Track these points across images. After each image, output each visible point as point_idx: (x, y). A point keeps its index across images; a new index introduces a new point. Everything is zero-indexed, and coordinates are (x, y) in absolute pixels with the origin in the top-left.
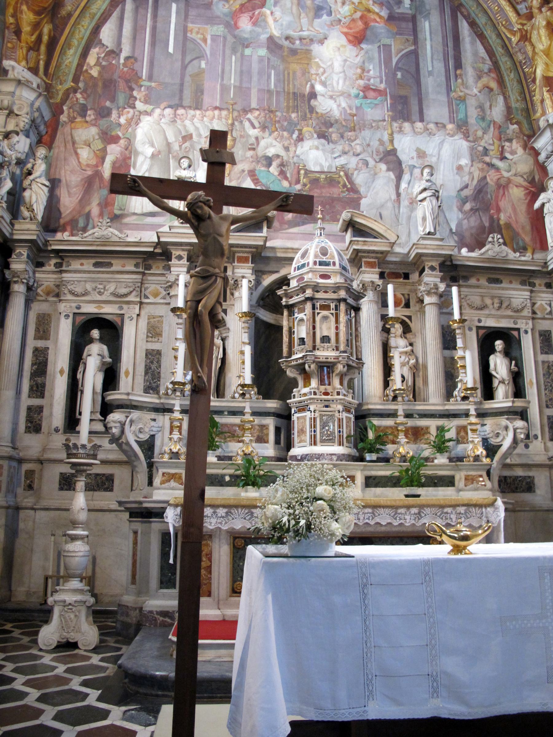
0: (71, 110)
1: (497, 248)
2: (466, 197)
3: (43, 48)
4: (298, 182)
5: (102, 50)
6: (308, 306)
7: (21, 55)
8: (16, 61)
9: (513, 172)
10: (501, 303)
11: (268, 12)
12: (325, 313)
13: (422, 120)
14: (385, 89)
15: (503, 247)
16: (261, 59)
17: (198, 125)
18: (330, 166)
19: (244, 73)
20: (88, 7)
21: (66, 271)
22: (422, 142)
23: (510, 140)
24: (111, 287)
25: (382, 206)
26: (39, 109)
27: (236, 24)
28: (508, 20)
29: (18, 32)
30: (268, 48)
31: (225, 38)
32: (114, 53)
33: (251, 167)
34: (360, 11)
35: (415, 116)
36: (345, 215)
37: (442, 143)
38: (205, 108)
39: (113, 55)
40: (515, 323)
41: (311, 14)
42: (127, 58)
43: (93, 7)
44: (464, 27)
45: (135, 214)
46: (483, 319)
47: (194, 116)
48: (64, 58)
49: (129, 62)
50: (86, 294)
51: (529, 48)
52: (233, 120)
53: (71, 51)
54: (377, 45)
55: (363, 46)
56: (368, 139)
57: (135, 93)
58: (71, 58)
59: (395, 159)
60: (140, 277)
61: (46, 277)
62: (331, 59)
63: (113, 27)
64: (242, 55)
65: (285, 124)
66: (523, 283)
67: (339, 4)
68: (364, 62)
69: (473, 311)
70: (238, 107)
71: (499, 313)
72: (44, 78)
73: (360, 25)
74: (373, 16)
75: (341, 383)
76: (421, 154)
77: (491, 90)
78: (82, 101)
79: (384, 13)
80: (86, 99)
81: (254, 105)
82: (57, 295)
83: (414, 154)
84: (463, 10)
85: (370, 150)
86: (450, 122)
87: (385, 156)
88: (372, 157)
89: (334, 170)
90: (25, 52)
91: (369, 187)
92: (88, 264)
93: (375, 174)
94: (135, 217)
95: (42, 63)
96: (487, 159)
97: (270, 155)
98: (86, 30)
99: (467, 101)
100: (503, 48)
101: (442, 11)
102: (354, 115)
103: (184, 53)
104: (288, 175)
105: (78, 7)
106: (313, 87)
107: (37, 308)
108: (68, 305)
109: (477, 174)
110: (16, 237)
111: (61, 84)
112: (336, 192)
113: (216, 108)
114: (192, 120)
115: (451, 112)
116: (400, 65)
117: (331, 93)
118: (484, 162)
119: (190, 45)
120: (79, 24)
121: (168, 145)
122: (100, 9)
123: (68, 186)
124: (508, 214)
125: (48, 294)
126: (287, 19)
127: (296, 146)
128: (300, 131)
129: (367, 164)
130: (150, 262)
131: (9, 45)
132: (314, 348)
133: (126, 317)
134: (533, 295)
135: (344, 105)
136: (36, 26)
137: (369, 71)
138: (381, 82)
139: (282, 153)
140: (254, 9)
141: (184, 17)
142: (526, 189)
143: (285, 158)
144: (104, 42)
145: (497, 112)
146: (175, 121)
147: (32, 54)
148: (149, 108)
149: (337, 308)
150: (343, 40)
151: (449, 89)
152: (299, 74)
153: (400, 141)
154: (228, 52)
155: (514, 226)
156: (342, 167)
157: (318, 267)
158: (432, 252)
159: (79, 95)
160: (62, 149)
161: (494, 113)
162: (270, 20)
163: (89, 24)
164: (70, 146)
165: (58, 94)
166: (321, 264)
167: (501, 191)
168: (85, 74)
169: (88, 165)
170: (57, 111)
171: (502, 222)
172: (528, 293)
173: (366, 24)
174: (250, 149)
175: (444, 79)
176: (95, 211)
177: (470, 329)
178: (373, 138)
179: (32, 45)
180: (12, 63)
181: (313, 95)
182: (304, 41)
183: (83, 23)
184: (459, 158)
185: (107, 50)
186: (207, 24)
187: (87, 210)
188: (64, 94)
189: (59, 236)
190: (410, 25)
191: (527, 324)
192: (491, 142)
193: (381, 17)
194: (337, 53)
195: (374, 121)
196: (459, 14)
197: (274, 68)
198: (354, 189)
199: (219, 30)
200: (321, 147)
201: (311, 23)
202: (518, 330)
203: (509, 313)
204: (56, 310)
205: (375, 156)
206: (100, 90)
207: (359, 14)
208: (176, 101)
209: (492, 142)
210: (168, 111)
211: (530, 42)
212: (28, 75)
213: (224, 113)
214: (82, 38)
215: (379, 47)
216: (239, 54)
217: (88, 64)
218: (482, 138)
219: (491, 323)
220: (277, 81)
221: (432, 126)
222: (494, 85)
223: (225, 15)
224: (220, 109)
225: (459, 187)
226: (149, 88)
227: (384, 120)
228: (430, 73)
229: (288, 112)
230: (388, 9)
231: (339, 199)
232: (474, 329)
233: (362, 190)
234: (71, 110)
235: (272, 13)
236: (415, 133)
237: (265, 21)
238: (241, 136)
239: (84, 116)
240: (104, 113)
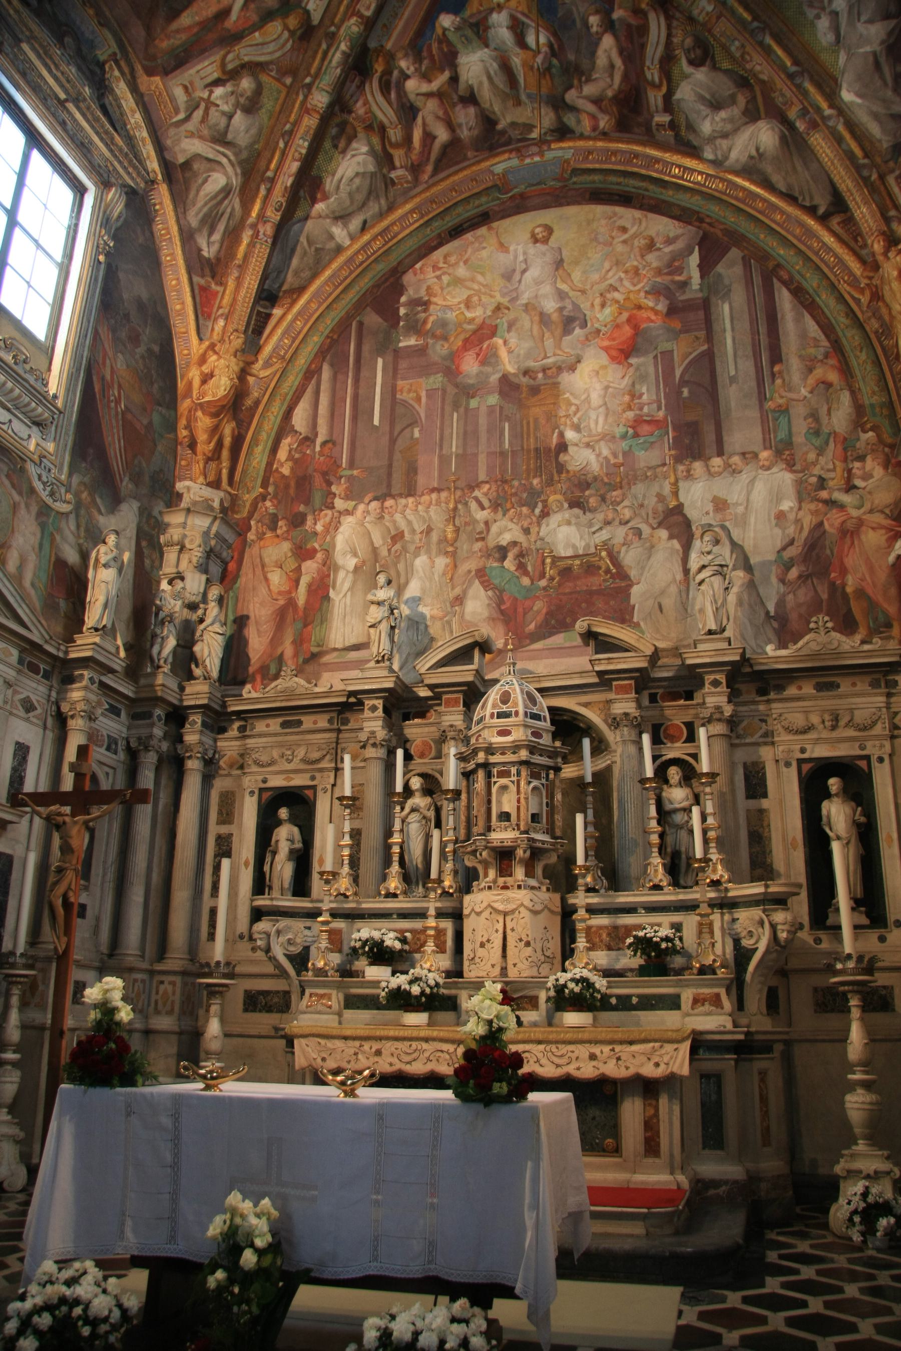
1: (822, 638)
2: (791, 559)
3: (225, 454)
4: (542, 575)
6: (481, 774)
9: (868, 506)
10: (836, 719)
11: (500, 342)
12: (503, 781)
13: (720, 453)
14: (666, 418)
15: (835, 635)
16: (491, 409)
17: (411, 517)
18: (587, 546)
19: (469, 435)
21: (249, 737)
22: (722, 487)
23: (861, 458)
24: (301, 753)
25: (663, 592)
26: (218, 535)
27: (458, 368)
28: (851, 273)
29: (193, 445)
30: (501, 393)
31: (444, 391)
32: (308, 440)
33: (481, 565)
34: (626, 310)
35: (711, 448)
36: (581, 625)
37: (752, 481)
38: (419, 493)
40: (862, 748)
41: (559, 331)
42: (324, 444)
44: (785, 299)
45: (335, 650)
46: (808, 747)
47: (406, 506)
49: (326, 451)
50: (272, 763)
51: (884, 311)
52: (456, 502)
53: (260, 448)
54: (651, 356)
55: (633, 361)
56: (640, 497)
57: (334, 488)
58: (259, 457)
59: (681, 519)
60: (334, 735)
61: (229, 745)
62: (586, 390)
63: (307, 406)
64: (467, 409)
65: (525, 495)
66: (875, 684)
67: (597, 308)
68: (633, 384)
69: (791, 737)
70: (461, 484)
71: (834, 734)
73: (628, 331)
74: (644, 314)
75: (529, 873)
76: (720, 505)
77: (829, 385)
78: (272, 510)
79: (662, 306)
80: (276, 506)
81: (482, 476)
82: (242, 767)
83: (710, 507)
84: (782, 273)
85: (643, 512)
86: (765, 448)
87: (665, 518)
88: (647, 522)
89: (593, 550)
91: (643, 568)
92: (274, 724)
93: (652, 547)
94: (335, 654)
95: (225, 472)
96: (824, 494)
97: (504, 543)
99: (791, 411)
100: (847, 315)
101: (749, 282)
102: (617, 466)
103: (392, 424)
104: (529, 568)
106: (561, 435)
107: (219, 785)
108: (253, 778)
109: (808, 521)
110: (186, 703)
112: (596, 582)
113: (433, 490)
114: (403, 513)
115: (766, 431)
116: (686, 378)
117: (586, 440)
118: (818, 500)
119: (400, 410)
121: (375, 551)
123: (257, 623)
124: (859, 575)
125: (231, 766)
126: (527, 345)
127: (539, 525)
128: (545, 502)
129: (638, 533)
130: (348, 715)
132: (489, 829)
133: (319, 788)
134: (893, 700)
135: (605, 452)
136: (215, 430)
137: (641, 395)
138: (659, 408)
139: (521, 538)
140: (481, 341)
141: (393, 373)
142: (889, 529)
143: (525, 545)
144: (297, 428)
145: (840, 417)
146: (381, 518)
147: (213, 465)
148: (350, 504)
149: (519, 774)
150: (604, 359)
151: (762, 398)
152: (542, 421)
153: (688, 491)
154: (448, 409)
155: (870, 591)
156: (605, 543)
157: (496, 720)
158: (707, 660)
159: (268, 504)
160: (251, 576)
161: (834, 420)
162: (503, 353)
164: (259, 571)
166: (500, 715)
167: (848, 540)
169: (280, 593)
170: (241, 530)
171: (849, 590)
172: (883, 699)
173: (636, 328)
174: (477, 540)
175: (753, 384)
176: (288, 650)
177: (788, 764)
178: (648, 494)
180: (187, 483)
181: (563, 447)
182: (549, 372)
184: (779, 500)
186: (420, 376)
187: (279, 651)
189: (247, 691)
190: (701, 314)
191: (882, 746)
192: (831, 466)
193: (656, 313)
194: (595, 380)
195: (649, 468)
196: (775, 280)
197: (508, 419)
198: (622, 574)
199: (437, 380)
200: (573, 521)
201: (558, 345)
202: (867, 758)
203: (851, 733)
204: (240, 786)
205: (651, 520)
206: (292, 491)
207: (625, 315)
208: (383, 489)
209: (831, 466)
210: (374, 505)
211: (884, 301)
212: (208, 492)
213: (444, 495)
215: (655, 357)
216: (462, 410)
218: (814, 464)
219: (822, 752)
220: (513, 436)
221: (736, 459)
222: (833, 377)
223: (444, 358)
224: (439, 490)
225: (779, 545)
226: (350, 478)
227: (664, 464)
228: (733, 380)
229: (527, 479)
230: (667, 298)
231: (600, 592)
232: (794, 764)
233: (633, 574)
235: (505, 342)
236: (711, 474)
237: (496, 355)
238: (466, 524)
239: (273, 527)
240: (297, 521)
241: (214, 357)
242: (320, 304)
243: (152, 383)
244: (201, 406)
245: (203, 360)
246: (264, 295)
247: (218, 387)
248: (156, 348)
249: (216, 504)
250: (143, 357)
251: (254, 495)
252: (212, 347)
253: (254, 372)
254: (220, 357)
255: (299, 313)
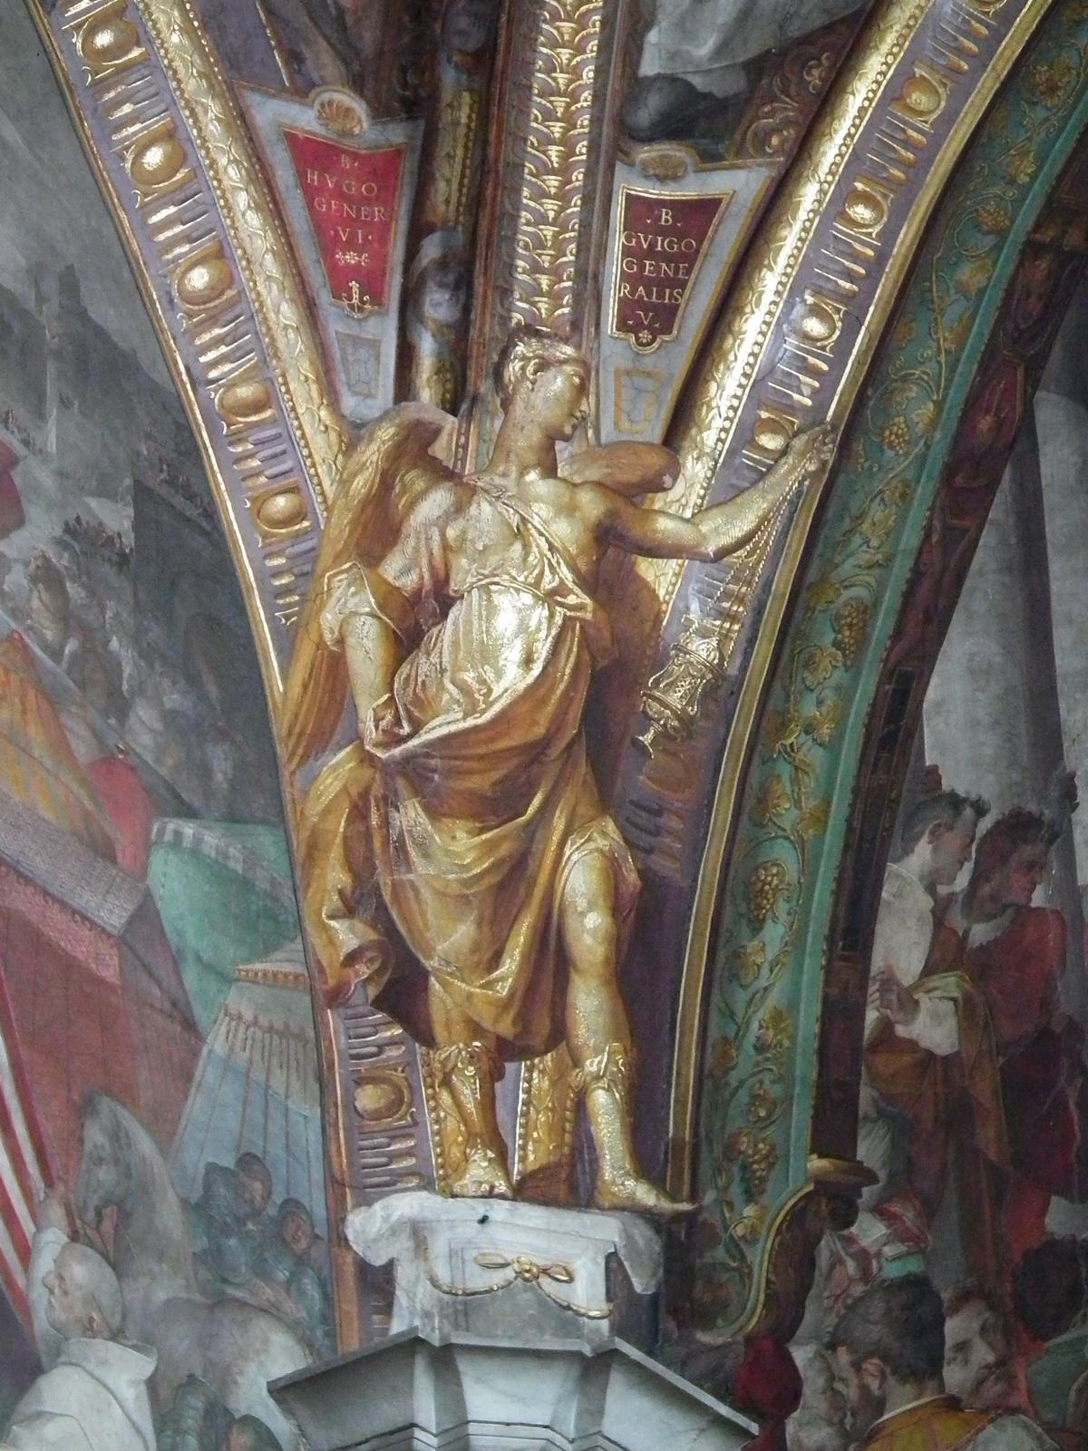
0: (843, 1356)
3: (589, 1004)
5: (952, 841)
7: (452, 1124)
8: (427, 1185)
20: (823, 579)
29: (403, 992)
39: (1028, 851)
43: (847, 567)
48: (741, 997)
53: (775, 933)
63: (991, 650)
72: (645, 1195)
80: (914, 1242)
90: (469, 1094)
95: (605, 1108)
98: (833, 746)
105: (759, 611)
111: (750, 1196)
120: (783, 727)
122: (890, 559)
131: (368, 1098)
136: (512, 883)
144: (956, 780)
159: (869, 1231)
163: (845, 693)
165: (745, 1274)
168: (883, 1063)
179: (506, 1028)
183: (809, 709)
185: (986, 824)
188: (781, 1254)
206: (989, 1137)
212: (527, 1234)
214: (821, 817)
217: (889, 982)
234: (843, 1356)
241: (437, 501)
242: (961, 86)
243: (119, 706)
244: (414, 772)
245: (378, 528)
246: (649, 110)
247: (487, 655)
248: (117, 518)
249: (587, 1293)
250: (46, 575)
251: (786, 1191)
252: (415, 447)
253: (665, 526)
254: (466, 493)
255: (855, 163)
